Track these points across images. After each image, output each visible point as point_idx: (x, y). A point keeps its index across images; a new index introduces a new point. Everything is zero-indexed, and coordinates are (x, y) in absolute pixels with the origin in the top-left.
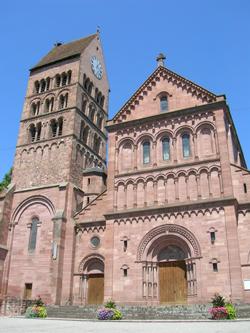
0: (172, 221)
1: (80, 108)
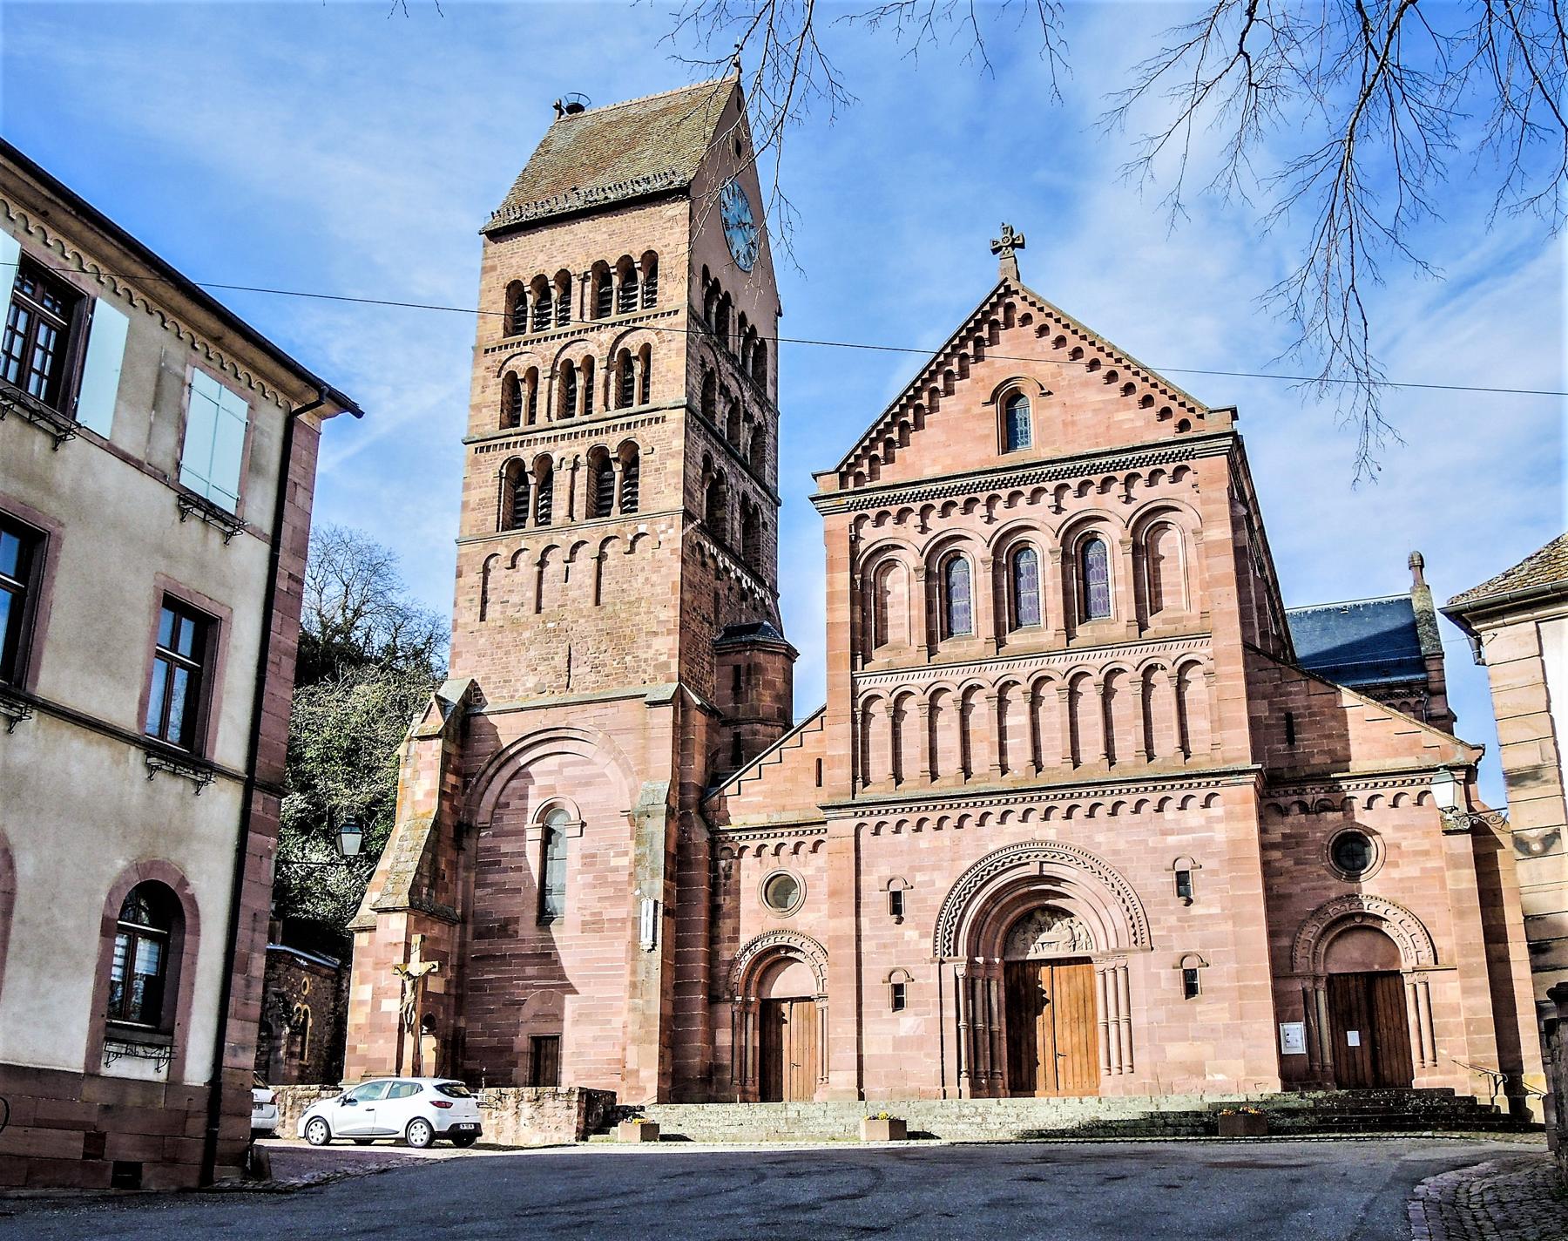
0: (1051, 831)
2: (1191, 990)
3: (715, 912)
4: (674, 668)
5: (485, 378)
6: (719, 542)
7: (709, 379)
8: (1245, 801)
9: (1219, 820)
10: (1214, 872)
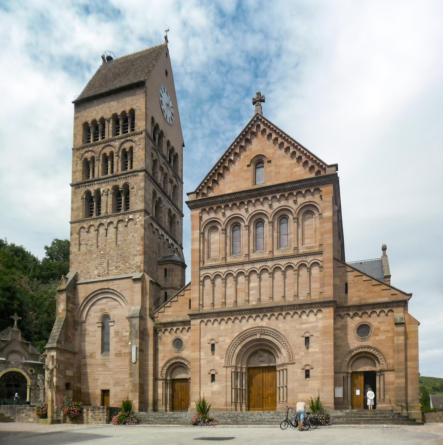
2: (307, 375)
7: (155, 162)
8: (330, 312)
10: (318, 337)
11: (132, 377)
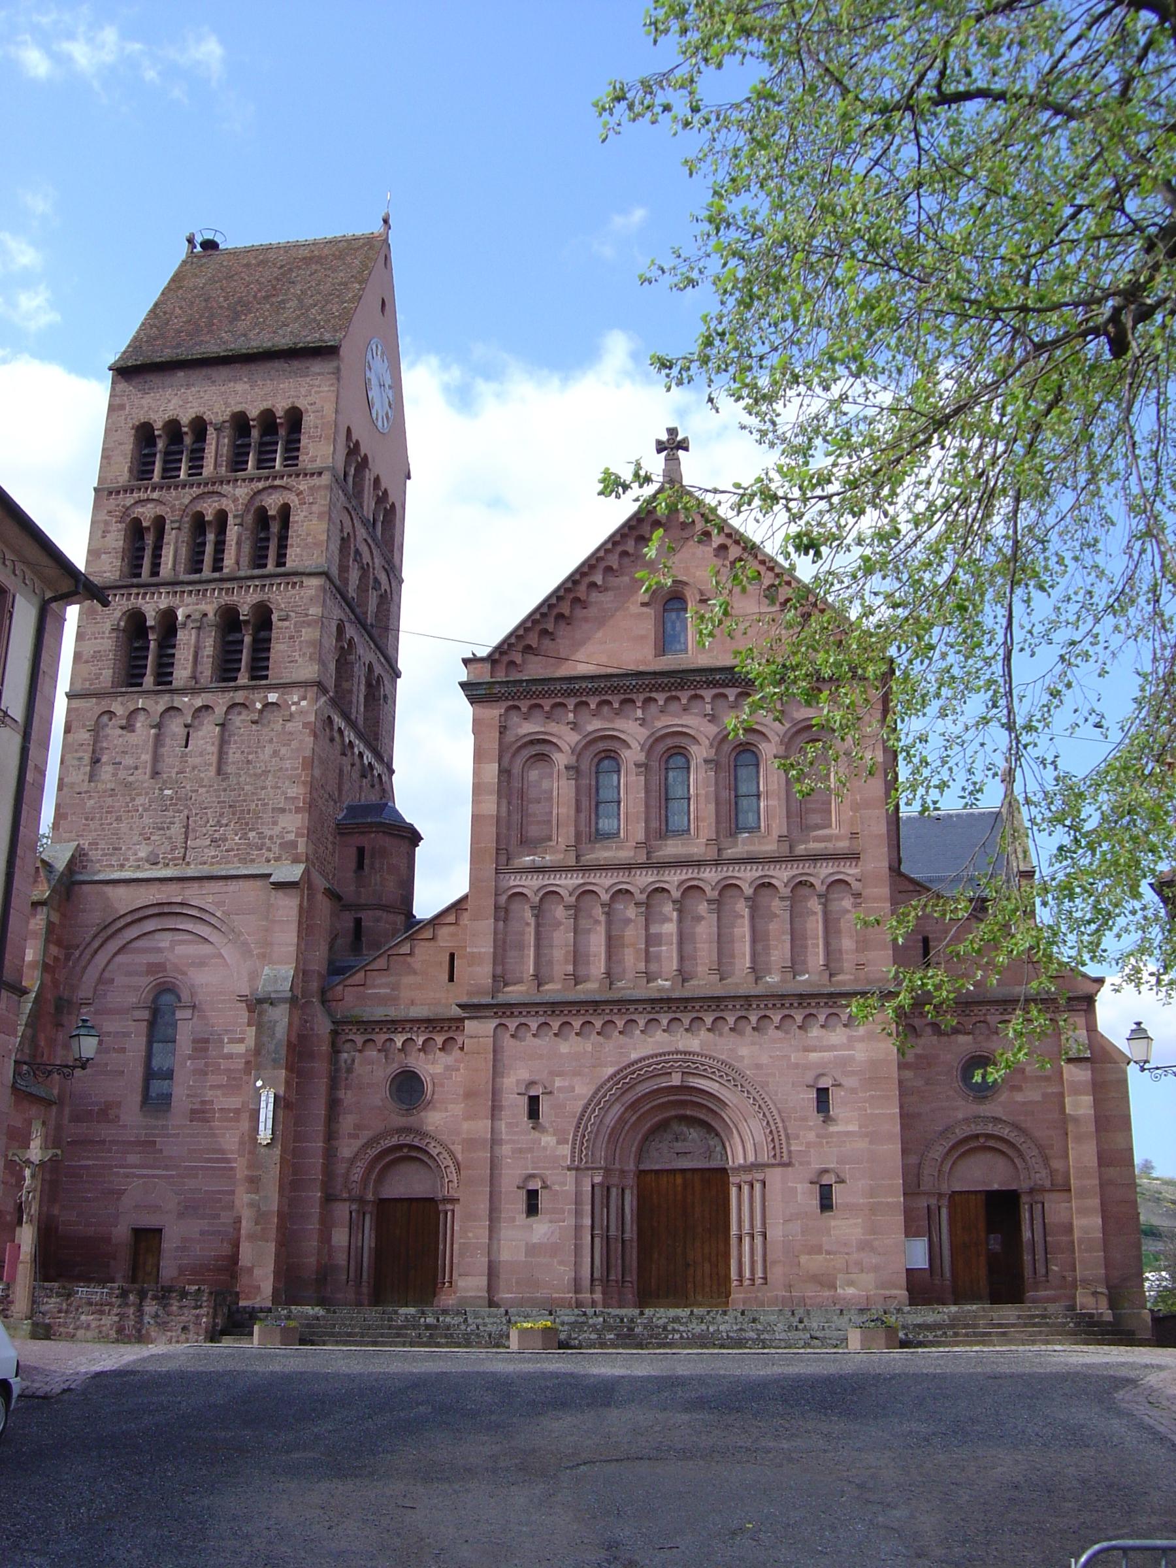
1: (334, 572)
2: (826, 1204)
3: (334, 1106)
4: (301, 848)
5: (106, 523)
6: (346, 716)
7: (345, 541)
9: (861, 1039)
10: (853, 1091)
11: (257, 1191)
